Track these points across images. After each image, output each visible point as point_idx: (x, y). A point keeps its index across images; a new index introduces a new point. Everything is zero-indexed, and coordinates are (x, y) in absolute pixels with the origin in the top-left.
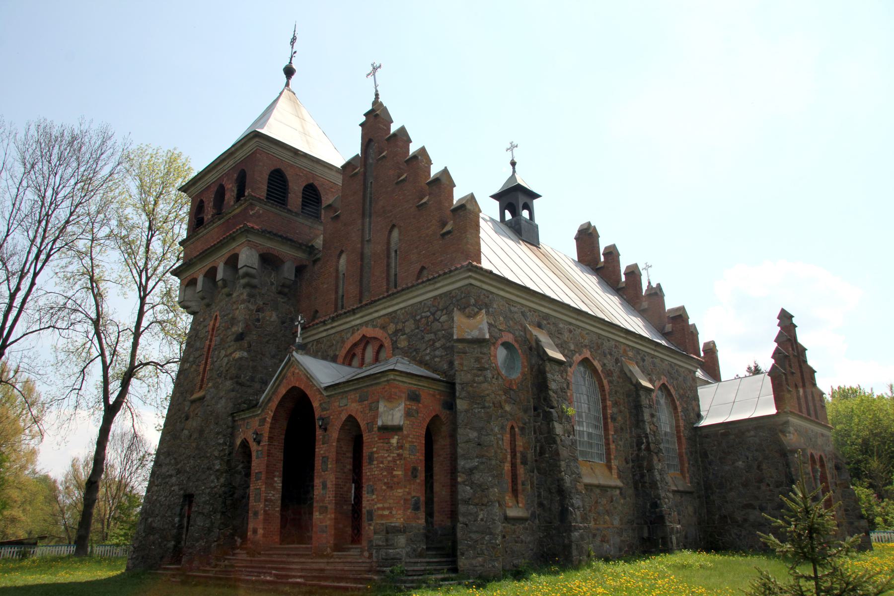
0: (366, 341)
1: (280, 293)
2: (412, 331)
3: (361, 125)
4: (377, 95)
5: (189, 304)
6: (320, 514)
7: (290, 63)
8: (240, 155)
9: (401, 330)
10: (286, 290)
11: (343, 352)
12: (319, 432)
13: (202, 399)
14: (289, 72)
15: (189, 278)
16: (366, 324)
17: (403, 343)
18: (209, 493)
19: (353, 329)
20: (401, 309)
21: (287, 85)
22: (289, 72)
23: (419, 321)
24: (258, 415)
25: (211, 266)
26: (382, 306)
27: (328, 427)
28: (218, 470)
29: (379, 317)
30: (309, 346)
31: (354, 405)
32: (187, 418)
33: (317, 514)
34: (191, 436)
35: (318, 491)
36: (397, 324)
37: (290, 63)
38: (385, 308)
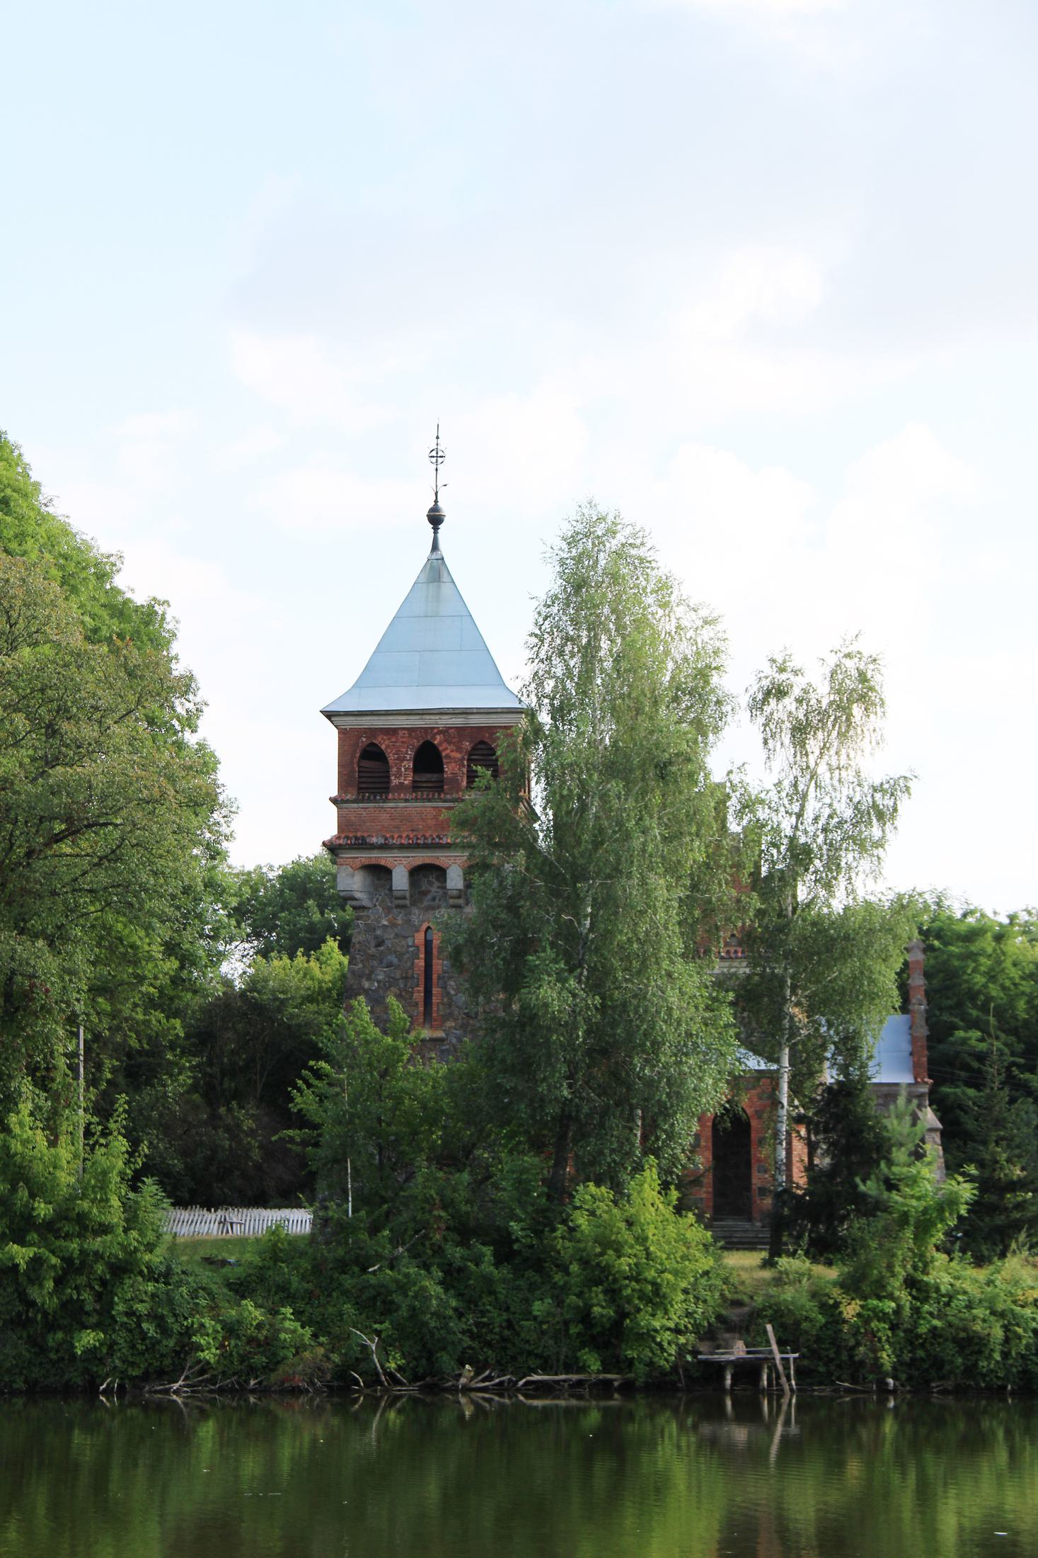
7: (436, 501)
8: (475, 721)
13: (441, 1040)
14: (435, 519)
37: (436, 501)
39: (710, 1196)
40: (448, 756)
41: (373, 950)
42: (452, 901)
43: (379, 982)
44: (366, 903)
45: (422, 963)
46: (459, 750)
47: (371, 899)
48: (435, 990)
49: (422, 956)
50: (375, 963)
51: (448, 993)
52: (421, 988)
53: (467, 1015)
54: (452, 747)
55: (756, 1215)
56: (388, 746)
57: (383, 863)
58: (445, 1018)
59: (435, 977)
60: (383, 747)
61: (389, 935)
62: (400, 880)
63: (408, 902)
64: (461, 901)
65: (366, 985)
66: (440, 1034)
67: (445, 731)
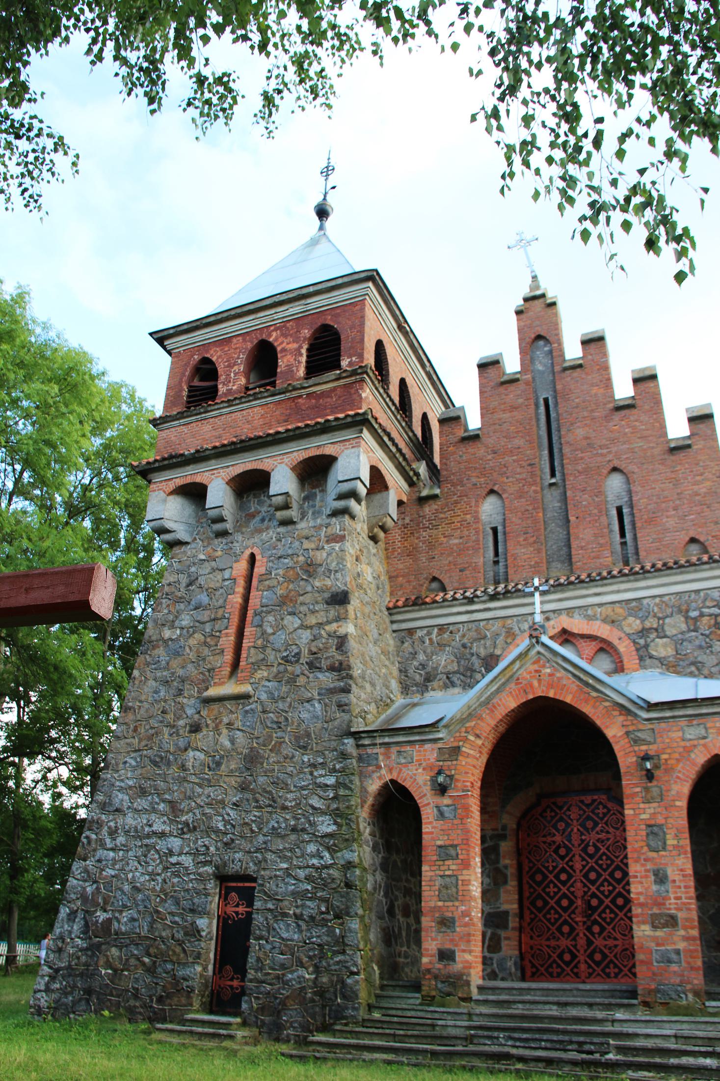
1: (374, 538)
2: (682, 633)
3: (519, 313)
4: (535, 278)
5: (169, 525)
6: (654, 927)
7: (325, 199)
8: (317, 303)
9: (656, 630)
10: (382, 535)
12: (631, 784)
13: (246, 697)
14: (322, 213)
15: (180, 482)
16: (569, 611)
17: (662, 648)
18: (308, 878)
20: (654, 597)
22: (322, 213)
23: (695, 619)
25: (249, 467)
27: (657, 773)
29: (600, 605)
30: (420, 633)
32: (195, 728)
34: (218, 764)
35: (641, 887)
36: (643, 619)
37: (325, 199)
38: (618, 592)
39: (697, 946)
40: (284, 350)
42: (280, 515)
43: (182, 628)
44: (182, 534)
47: (192, 534)
48: (248, 631)
51: (264, 633)
52: (232, 630)
53: (286, 659)
57: (198, 479)
58: (256, 666)
59: (250, 613)
63: (229, 526)
65: (167, 633)
66: (246, 688)
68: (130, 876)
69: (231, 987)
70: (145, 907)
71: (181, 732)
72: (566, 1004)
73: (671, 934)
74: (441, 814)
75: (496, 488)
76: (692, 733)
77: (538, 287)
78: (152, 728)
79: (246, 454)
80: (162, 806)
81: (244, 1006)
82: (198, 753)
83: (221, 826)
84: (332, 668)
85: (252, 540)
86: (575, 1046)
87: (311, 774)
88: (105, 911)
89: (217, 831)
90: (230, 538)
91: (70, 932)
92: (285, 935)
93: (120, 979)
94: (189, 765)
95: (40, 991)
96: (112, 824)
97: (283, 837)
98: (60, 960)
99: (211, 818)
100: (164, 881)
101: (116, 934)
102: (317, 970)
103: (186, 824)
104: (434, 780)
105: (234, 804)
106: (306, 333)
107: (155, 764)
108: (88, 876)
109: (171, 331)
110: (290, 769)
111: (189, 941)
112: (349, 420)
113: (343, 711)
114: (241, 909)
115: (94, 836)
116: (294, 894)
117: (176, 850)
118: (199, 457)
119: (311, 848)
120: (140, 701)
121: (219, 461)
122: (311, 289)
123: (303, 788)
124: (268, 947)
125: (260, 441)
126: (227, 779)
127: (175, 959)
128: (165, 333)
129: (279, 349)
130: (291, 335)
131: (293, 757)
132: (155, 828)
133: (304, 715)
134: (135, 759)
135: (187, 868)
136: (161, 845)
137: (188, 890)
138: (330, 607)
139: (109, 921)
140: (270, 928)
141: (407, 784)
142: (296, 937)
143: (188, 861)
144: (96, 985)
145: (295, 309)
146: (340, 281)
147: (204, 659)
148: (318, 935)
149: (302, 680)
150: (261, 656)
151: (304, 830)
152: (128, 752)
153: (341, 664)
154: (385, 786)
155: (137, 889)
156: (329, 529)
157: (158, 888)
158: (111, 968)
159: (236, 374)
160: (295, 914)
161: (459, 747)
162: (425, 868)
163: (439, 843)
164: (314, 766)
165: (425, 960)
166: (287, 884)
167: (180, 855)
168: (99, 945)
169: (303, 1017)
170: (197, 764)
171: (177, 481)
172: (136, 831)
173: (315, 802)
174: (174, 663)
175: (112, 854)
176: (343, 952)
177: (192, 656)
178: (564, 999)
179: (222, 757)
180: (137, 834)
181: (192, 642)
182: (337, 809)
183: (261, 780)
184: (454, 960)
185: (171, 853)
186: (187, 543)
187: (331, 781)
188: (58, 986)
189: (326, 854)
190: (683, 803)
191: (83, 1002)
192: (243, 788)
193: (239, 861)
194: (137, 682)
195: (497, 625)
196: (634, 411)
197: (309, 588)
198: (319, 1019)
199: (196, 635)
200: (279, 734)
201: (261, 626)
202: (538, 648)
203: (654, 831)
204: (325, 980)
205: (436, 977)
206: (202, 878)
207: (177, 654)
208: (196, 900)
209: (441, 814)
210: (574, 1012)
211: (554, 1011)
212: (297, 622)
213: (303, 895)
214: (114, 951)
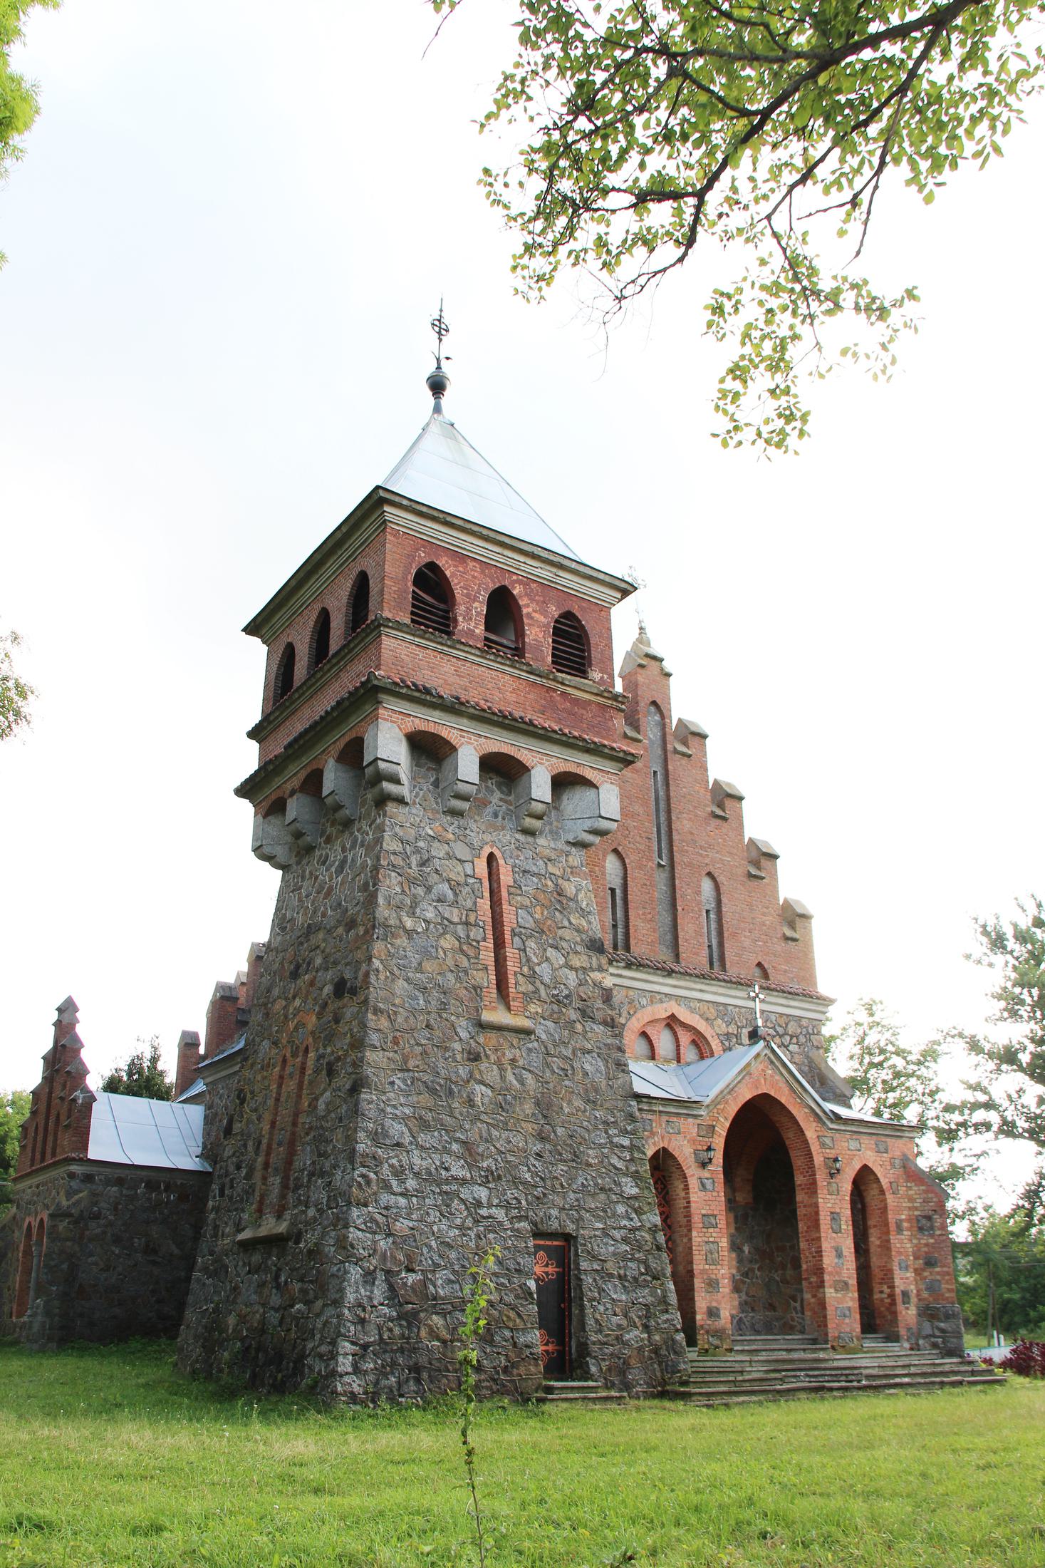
0: (672, 1022)
7: (439, 368)
11: (634, 1025)
12: (821, 1177)
13: (527, 1032)
14: (437, 386)
15: (423, 726)
18: (625, 1240)
19: (654, 997)
21: (437, 409)
22: (437, 386)
24: (695, 1116)
26: (714, 989)
28: (635, 1197)
31: (869, 1153)
32: (475, 1057)
33: (832, 1290)
35: (828, 1260)
37: (439, 368)
41: (414, 871)
45: (485, 904)
46: (544, 613)
48: (510, 952)
49: (487, 894)
50: (420, 891)
51: (528, 960)
54: (534, 605)
55: (903, 1332)
56: (453, 575)
58: (527, 997)
60: (448, 573)
61: (439, 850)
62: (467, 766)
64: (537, 824)
65: (409, 923)
67: (527, 581)
68: (435, 1228)
69: (547, 1351)
70: (463, 1266)
71: (459, 1057)
72: (791, 1350)
73: (844, 1296)
74: (703, 1185)
75: (620, 849)
76: (853, 1145)
77: (649, 645)
78: (418, 1044)
79: (505, 733)
80: (455, 1147)
81: (593, 1369)
82: (483, 1088)
83: (527, 1176)
84: (605, 1023)
85: (487, 838)
86: (843, 1378)
87: (606, 1133)
88: (413, 1271)
89: (525, 1183)
90: (462, 822)
91: (370, 1299)
92: (614, 1296)
93: (453, 1352)
94: (478, 1100)
95: (347, 1373)
96: (394, 1161)
97: (593, 1195)
98: (365, 1334)
99: (516, 1167)
100: (478, 1236)
101: (435, 1299)
102: (646, 1327)
103: (488, 1169)
104: (696, 1152)
105: (537, 1154)
106: (554, 611)
107: (433, 1092)
108: (373, 1227)
109: (405, 502)
110: (585, 1124)
111: (522, 1305)
112: (621, 755)
113: (623, 1071)
114: (550, 1269)
115: (372, 1176)
116: (614, 1254)
117: (484, 1200)
118: (455, 707)
119: (621, 1209)
120: (394, 1005)
121: (474, 724)
122: (573, 565)
123: (601, 1146)
124: (601, 1308)
125: (531, 728)
126: (523, 1124)
127: (511, 1325)
128: (397, 499)
129: (525, 611)
130: (537, 602)
131: (585, 1111)
132: (454, 1172)
133: (587, 1067)
134: (404, 1081)
135: (500, 1223)
136: (465, 1193)
137: (508, 1248)
138: (591, 953)
139: (424, 1283)
140: (601, 1290)
141: (676, 1154)
142: (624, 1297)
143: (500, 1214)
144: (423, 1361)
145: (545, 573)
146: (601, 576)
147: (466, 972)
148: (644, 1296)
149: (579, 1027)
150: (531, 988)
151: (611, 1189)
152: (393, 1070)
153: (612, 1019)
154: (656, 1154)
155: (450, 1246)
156: (570, 859)
157: (472, 1244)
158: (438, 1339)
159: (478, 614)
160: (620, 1276)
161: (714, 1127)
162: (694, 1234)
163: (704, 1212)
164: (606, 1123)
165: (698, 1317)
166: (606, 1244)
167: (490, 1206)
168: (415, 1314)
169: (646, 1374)
170: (486, 1100)
171: (417, 721)
172: (430, 1174)
173: (615, 1161)
174: (428, 966)
175: (402, 1201)
176: (667, 1311)
177: (450, 962)
178: (790, 1347)
179: (515, 1098)
180: (430, 1178)
181: (442, 942)
182: (637, 1172)
183: (560, 1131)
184: (719, 1316)
185: (479, 1204)
186: (407, 804)
187: (626, 1142)
188: (372, 1366)
189: (634, 1215)
190: (848, 1198)
191: (411, 1383)
192: (542, 1137)
193: (556, 1219)
194: (382, 977)
195: (624, 992)
196: (725, 824)
197: (566, 923)
198: (658, 1374)
199: (448, 936)
200: (567, 1083)
201: (525, 950)
202: (767, 1051)
203: (835, 1217)
204: (657, 1338)
205: (707, 1332)
206: (518, 1234)
207: (426, 954)
208: (521, 1261)
209: (703, 1185)
210: (795, 1355)
211: (784, 1355)
212: (562, 961)
213: (624, 1257)
214: (437, 1320)
